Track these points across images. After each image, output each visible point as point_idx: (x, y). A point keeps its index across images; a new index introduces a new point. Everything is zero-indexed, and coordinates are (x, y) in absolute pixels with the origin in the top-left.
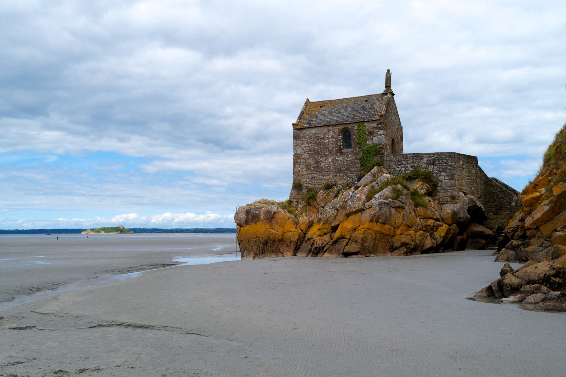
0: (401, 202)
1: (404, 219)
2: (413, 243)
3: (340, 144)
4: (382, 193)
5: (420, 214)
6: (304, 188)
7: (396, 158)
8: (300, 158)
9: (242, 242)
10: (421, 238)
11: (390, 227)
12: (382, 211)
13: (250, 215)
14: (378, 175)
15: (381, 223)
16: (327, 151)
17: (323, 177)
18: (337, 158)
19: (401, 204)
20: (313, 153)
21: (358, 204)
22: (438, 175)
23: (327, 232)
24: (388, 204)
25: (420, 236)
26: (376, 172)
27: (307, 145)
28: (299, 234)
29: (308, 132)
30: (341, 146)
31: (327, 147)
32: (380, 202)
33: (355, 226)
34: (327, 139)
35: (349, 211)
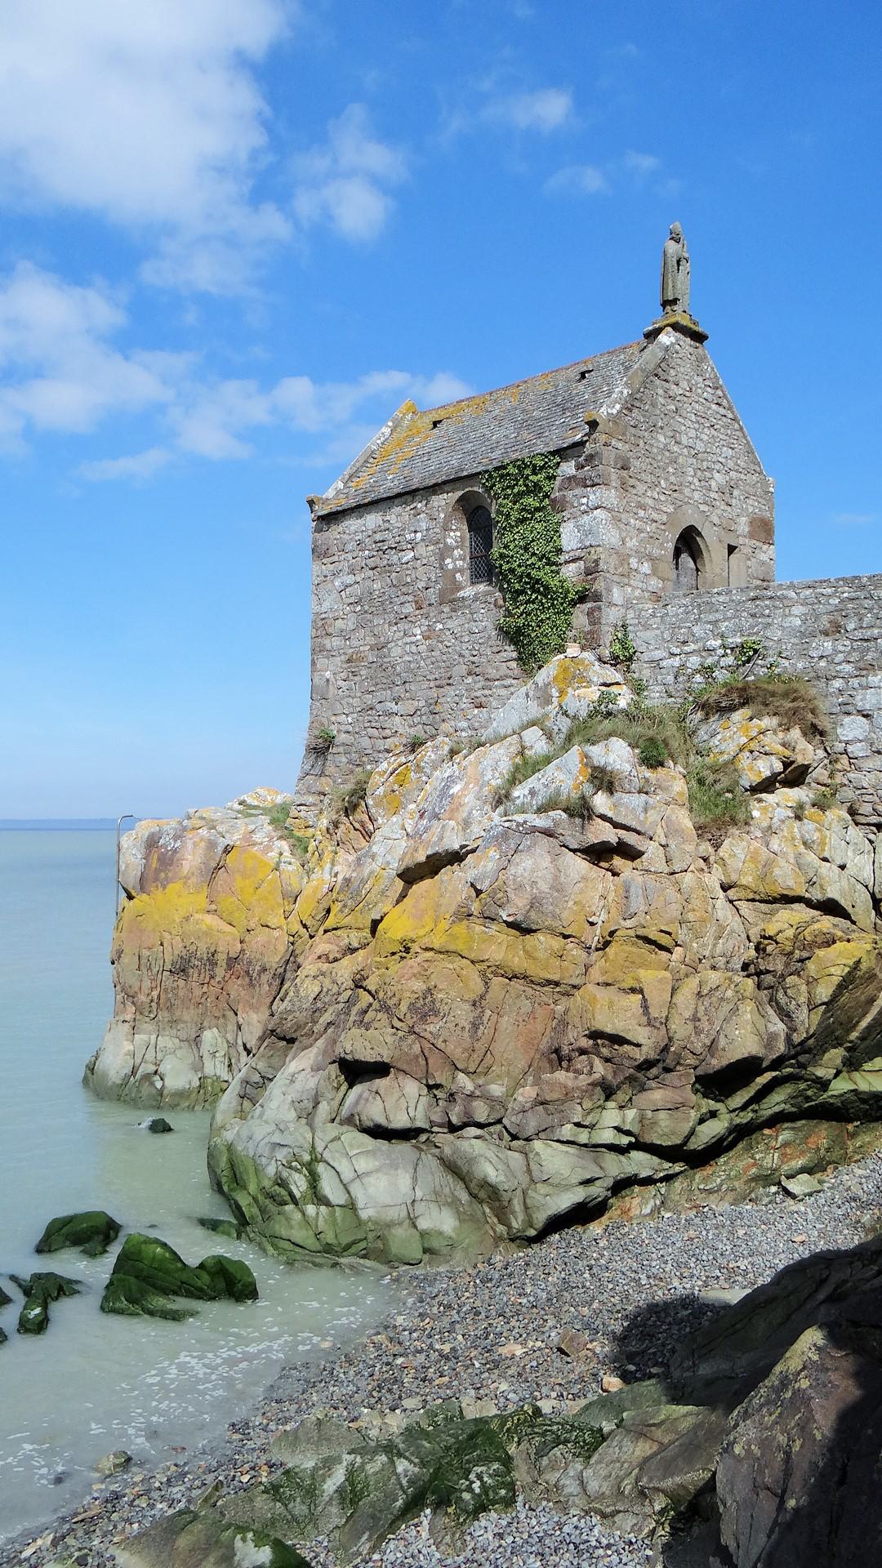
0: (616, 825)
1: (627, 906)
2: (641, 1034)
3: (450, 567)
4: (543, 781)
5: (734, 877)
6: (341, 749)
7: (667, 614)
8: (330, 630)
9: (119, 957)
10: (701, 1009)
11: (557, 943)
12: (512, 870)
13: (156, 857)
14: (562, 693)
15: (510, 925)
16: (410, 598)
17: (396, 704)
18: (440, 626)
19: (610, 835)
20: (366, 606)
21: (443, 826)
22: (855, 682)
23: (355, 945)
24: (548, 833)
25: (699, 995)
26: (555, 678)
27: (350, 579)
28: (291, 939)
29: (352, 524)
30: (458, 575)
31: (409, 580)
32: (507, 824)
33: (412, 935)
34: (409, 546)
35: (408, 856)
